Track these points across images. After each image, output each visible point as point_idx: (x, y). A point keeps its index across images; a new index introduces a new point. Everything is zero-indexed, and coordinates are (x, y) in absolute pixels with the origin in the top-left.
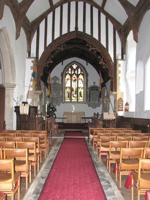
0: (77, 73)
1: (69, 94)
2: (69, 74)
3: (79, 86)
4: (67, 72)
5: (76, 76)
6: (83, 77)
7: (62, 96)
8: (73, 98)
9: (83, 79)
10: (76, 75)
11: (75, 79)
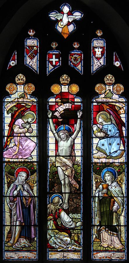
0: (79, 67)
1: (26, 210)
2: (31, 77)
3: (97, 157)
4: (12, 63)
5: (75, 89)
8: (55, 238)
10: (75, 78)
11: (68, 106)
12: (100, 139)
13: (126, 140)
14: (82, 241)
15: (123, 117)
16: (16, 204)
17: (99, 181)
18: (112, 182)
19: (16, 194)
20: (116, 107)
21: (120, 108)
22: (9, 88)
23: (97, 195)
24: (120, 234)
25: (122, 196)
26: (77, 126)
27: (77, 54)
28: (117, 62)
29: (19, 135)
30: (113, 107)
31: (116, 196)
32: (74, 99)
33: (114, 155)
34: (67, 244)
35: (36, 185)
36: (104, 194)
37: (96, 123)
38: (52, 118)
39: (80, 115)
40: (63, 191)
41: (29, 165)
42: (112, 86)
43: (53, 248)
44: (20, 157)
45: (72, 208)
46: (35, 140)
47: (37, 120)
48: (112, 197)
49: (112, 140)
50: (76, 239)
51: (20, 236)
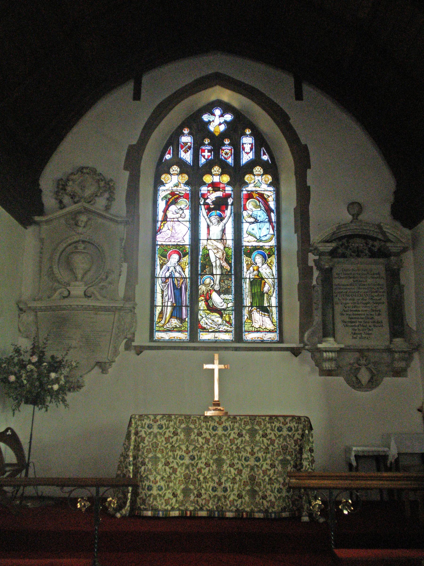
0: (230, 161)
1: (177, 291)
3: (248, 241)
4: (168, 157)
5: (226, 178)
6: (275, 183)
7: (129, 298)
8: (206, 319)
9: (269, 193)
10: (225, 169)
11: (219, 194)
12: (250, 224)
13: (275, 225)
14: (233, 322)
15: (272, 205)
16: (168, 285)
17: (249, 263)
18: (263, 264)
19: (168, 276)
20: (265, 196)
21: (269, 196)
22: (164, 178)
23: (248, 277)
24: (272, 315)
25: (273, 277)
26: (228, 212)
27: (228, 149)
28: (265, 156)
29: (172, 220)
30: (261, 195)
31: (266, 277)
32: (225, 187)
33: (264, 239)
34: (219, 325)
35: (188, 266)
36: (255, 275)
37: (245, 209)
38: (204, 205)
39: (231, 202)
40: (214, 273)
41: (181, 248)
42: (260, 177)
43: (204, 328)
44: (173, 240)
45: (224, 289)
46: (188, 224)
47: (190, 206)
48: (262, 279)
49: (262, 224)
50: (227, 319)
51: (171, 317)
